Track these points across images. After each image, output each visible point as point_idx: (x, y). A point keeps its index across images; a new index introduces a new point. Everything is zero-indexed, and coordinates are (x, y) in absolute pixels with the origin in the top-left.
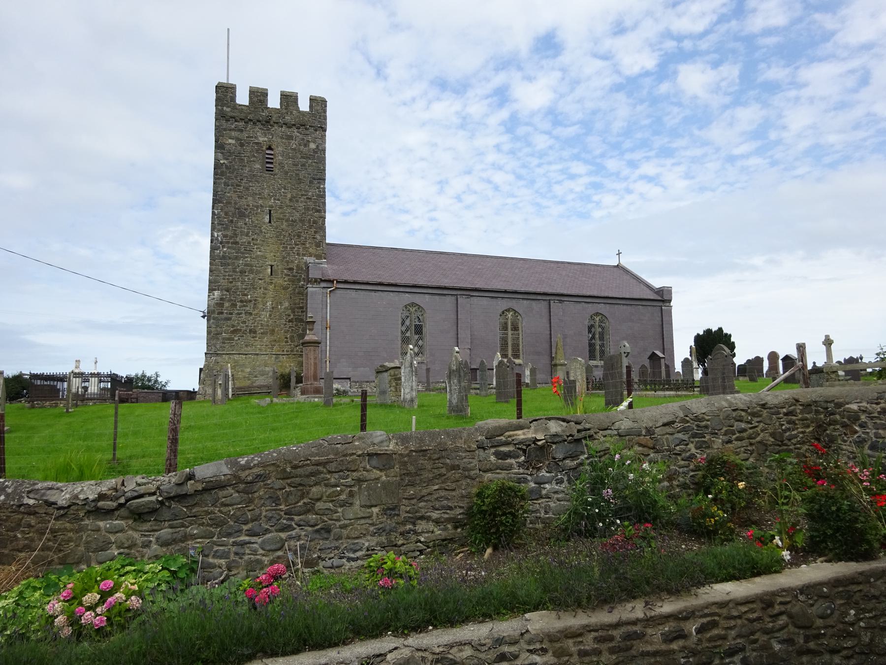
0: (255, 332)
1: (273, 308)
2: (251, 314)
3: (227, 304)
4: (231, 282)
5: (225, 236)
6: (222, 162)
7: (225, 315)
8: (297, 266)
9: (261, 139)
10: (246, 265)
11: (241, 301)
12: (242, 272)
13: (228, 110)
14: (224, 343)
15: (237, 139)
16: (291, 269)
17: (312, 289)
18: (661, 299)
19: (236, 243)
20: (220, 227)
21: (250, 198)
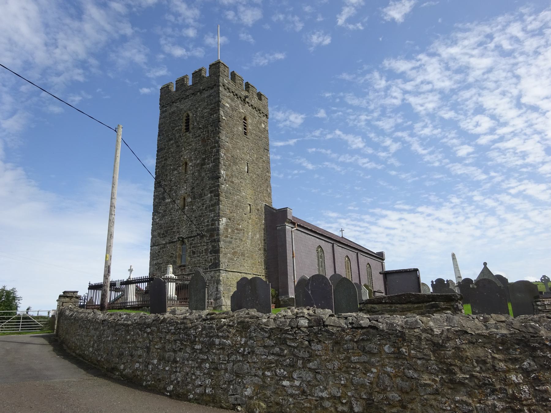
0: (244, 256)
1: (252, 238)
2: (241, 240)
3: (230, 230)
4: (231, 213)
5: (227, 175)
6: (224, 118)
7: (228, 239)
8: (261, 208)
9: (242, 111)
10: (238, 201)
11: (237, 229)
12: (237, 206)
13: (226, 82)
14: (229, 262)
15: (231, 106)
16: (258, 210)
17: (288, 227)
18: (380, 257)
19: (232, 182)
20: (224, 167)
21: (238, 151)
